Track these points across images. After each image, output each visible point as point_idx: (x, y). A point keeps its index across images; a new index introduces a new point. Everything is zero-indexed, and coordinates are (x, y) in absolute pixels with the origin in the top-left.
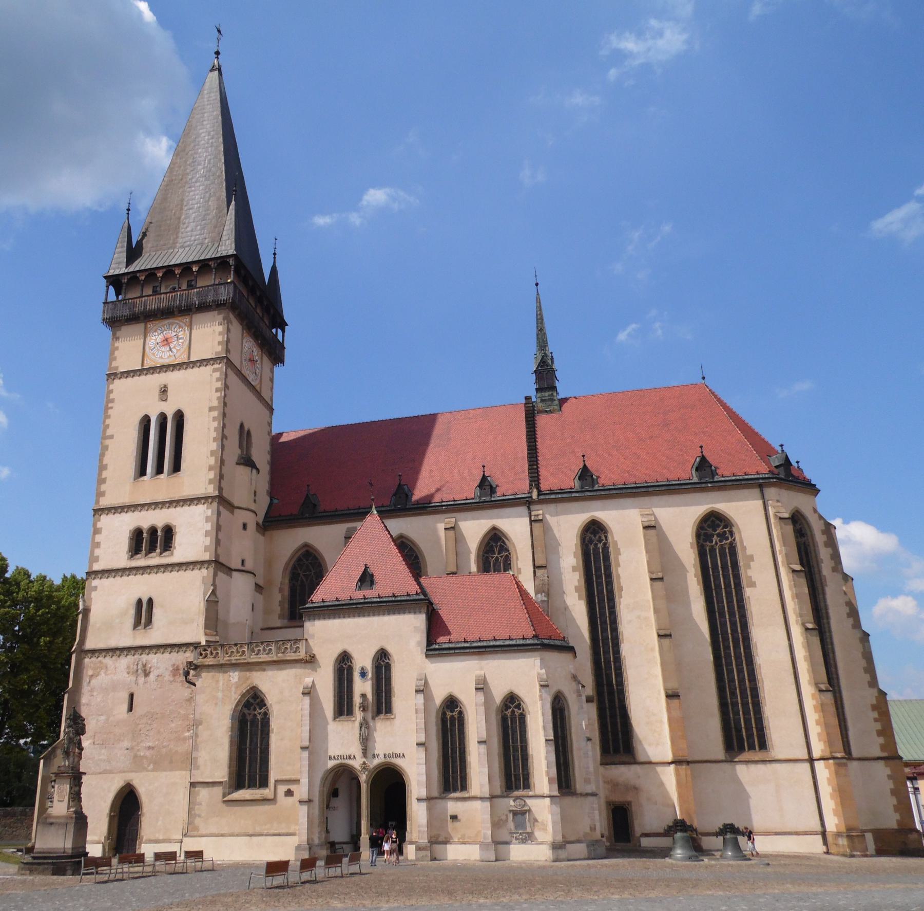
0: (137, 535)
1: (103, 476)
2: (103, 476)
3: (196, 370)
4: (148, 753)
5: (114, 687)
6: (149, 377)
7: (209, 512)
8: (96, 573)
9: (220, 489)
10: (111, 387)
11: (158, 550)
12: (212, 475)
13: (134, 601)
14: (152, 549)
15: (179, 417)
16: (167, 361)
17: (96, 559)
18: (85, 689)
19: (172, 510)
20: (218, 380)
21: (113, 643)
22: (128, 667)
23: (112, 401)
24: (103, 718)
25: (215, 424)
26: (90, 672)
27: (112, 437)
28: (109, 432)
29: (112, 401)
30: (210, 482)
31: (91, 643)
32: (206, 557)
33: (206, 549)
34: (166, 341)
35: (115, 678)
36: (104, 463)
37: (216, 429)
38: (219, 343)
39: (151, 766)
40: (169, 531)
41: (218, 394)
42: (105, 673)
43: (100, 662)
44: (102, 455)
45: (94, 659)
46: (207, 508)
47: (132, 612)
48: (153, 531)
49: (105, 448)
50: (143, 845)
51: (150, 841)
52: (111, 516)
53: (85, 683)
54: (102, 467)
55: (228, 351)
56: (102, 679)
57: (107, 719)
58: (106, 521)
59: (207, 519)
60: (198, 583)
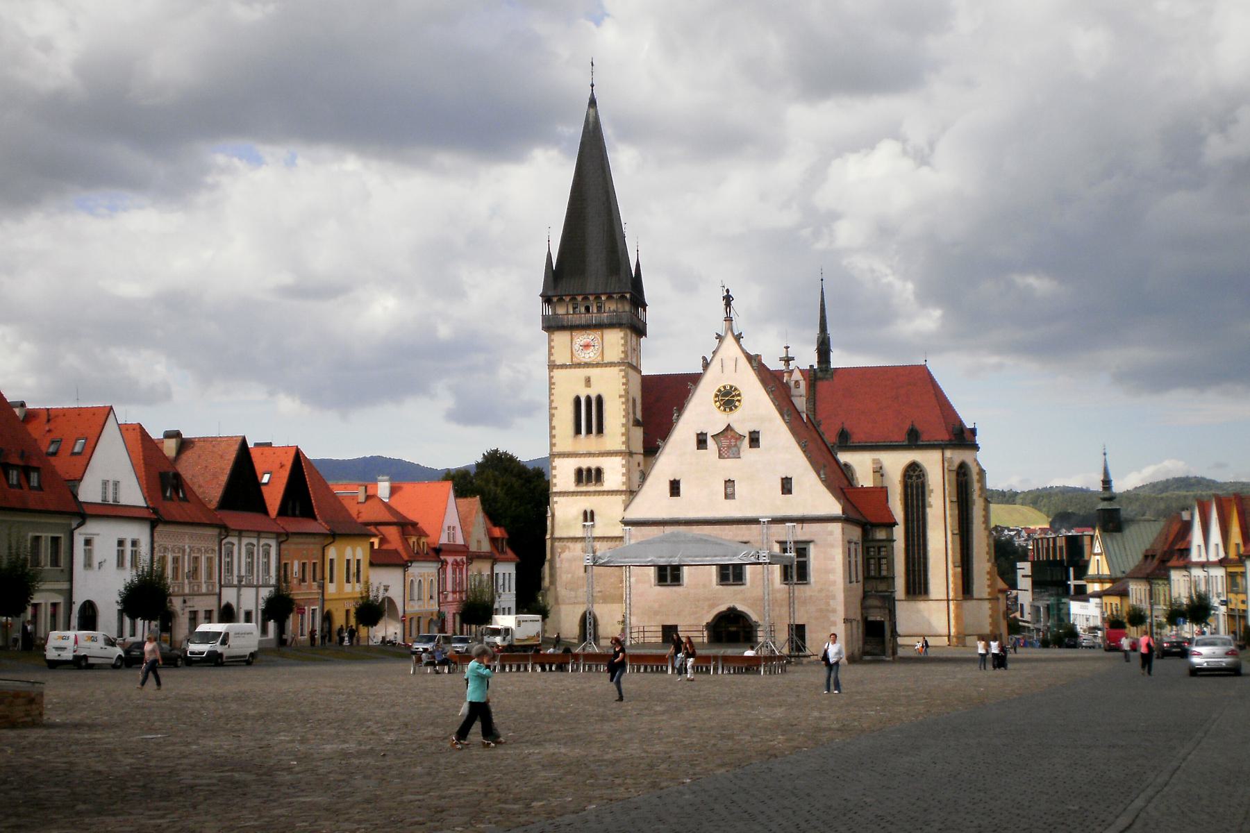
0: (579, 472)
1: (553, 433)
2: (553, 433)
3: (608, 369)
4: (599, 594)
5: (574, 559)
6: (578, 370)
7: (624, 462)
8: (556, 493)
9: (628, 446)
10: (552, 374)
11: (594, 482)
12: (624, 439)
13: (583, 512)
14: (589, 480)
15: (600, 400)
16: (587, 360)
17: (555, 485)
18: (557, 559)
19: (600, 458)
20: (623, 377)
21: (571, 535)
22: (582, 549)
23: (554, 384)
24: (570, 576)
25: (624, 406)
26: (559, 550)
27: (556, 408)
28: (554, 405)
29: (554, 384)
30: (623, 443)
31: (557, 535)
32: (624, 488)
33: (624, 483)
34: (587, 346)
35: (575, 554)
36: (553, 425)
37: (624, 410)
38: (622, 352)
39: (601, 601)
40: (599, 471)
41: (624, 387)
42: (569, 551)
43: (565, 545)
44: (551, 420)
45: (560, 543)
46: (623, 459)
47: (581, 518)
48: (589, 470)
49: (552, 416)
50: (601, 640)
51: (602, 638)
52: (561, 459)
53: (557, 557)
54: (552, 428)
55: (626, 356)
56: (566, 555)
57: (572, 577)
58: (557, 462)
59: (623, 466)
60: (621, 502)
